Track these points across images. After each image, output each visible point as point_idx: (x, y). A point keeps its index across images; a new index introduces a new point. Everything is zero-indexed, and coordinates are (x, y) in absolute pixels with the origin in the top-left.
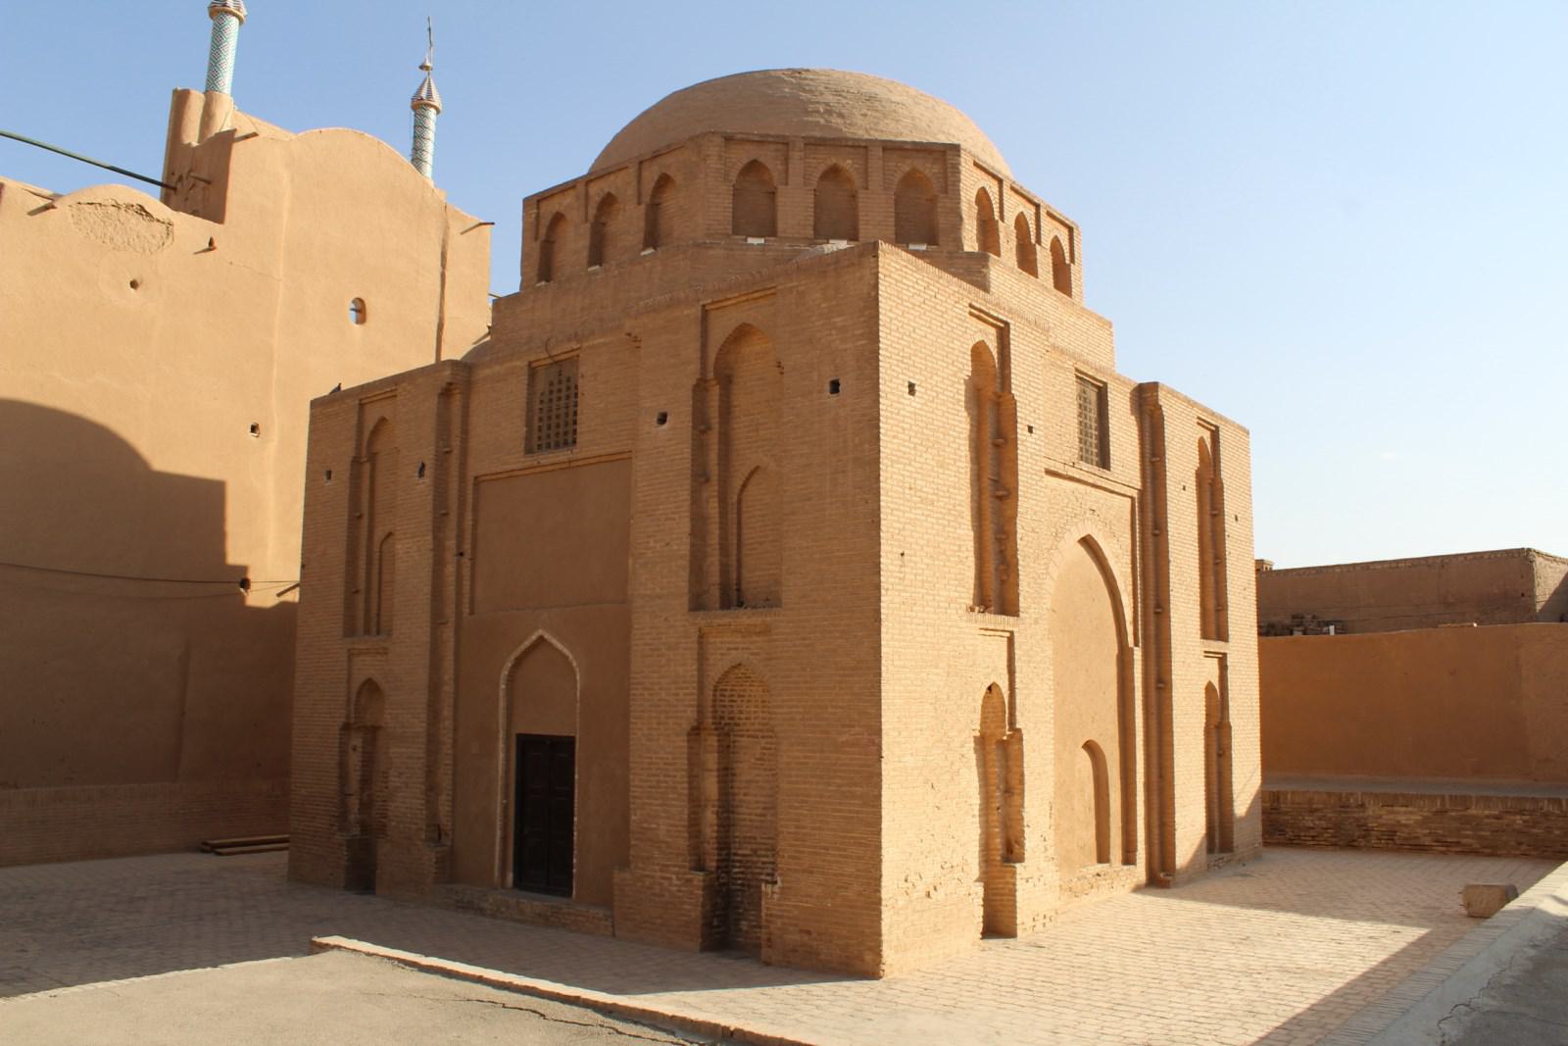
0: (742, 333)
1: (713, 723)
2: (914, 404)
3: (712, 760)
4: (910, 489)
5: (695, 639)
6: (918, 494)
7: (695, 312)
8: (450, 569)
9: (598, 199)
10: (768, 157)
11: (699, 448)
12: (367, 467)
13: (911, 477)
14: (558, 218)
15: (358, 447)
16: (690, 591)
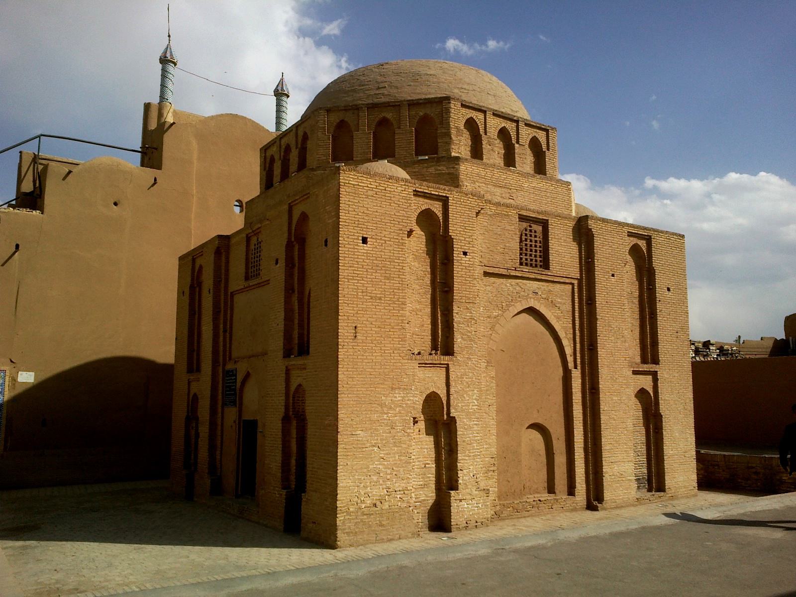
0: (304, 217)
1: (293, 414)
2: (365, 248)
3: (294, 432)
4: (363, 292)
5: (284, 372)
6: (369, 294)
7: (286, 207)
8: (221, 339)
9: (284, 147)
10: (349, 118)
11: (289, 275)
12: (197, 289)
13: (363, 286)
14: (272, 160)
15: (192, 279)
16: (284, 348)
